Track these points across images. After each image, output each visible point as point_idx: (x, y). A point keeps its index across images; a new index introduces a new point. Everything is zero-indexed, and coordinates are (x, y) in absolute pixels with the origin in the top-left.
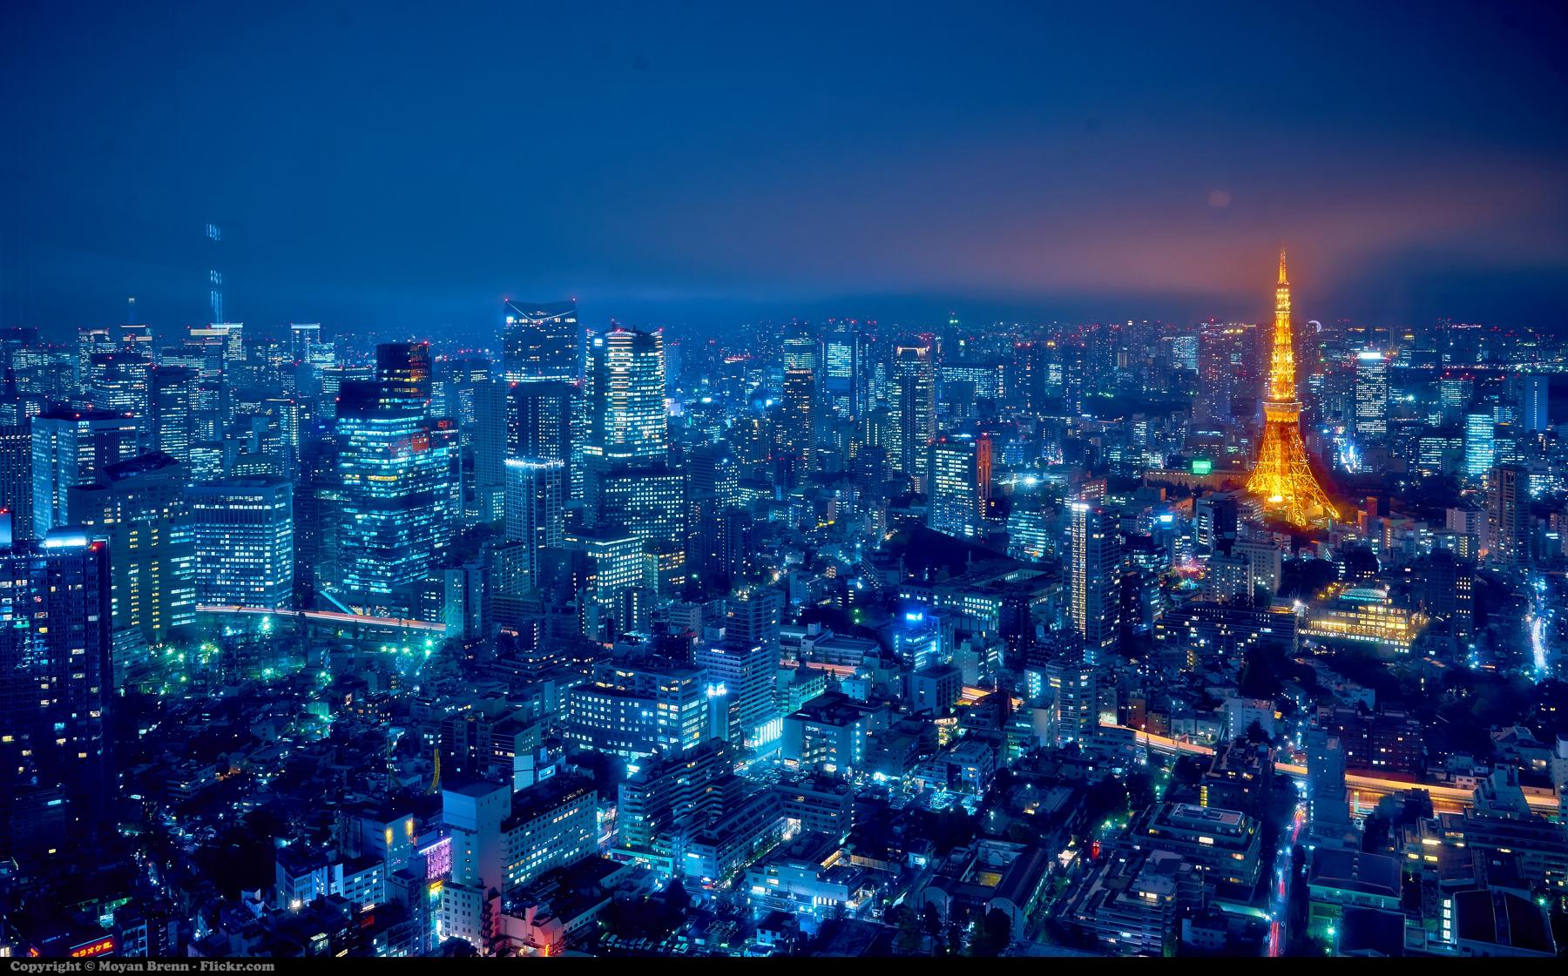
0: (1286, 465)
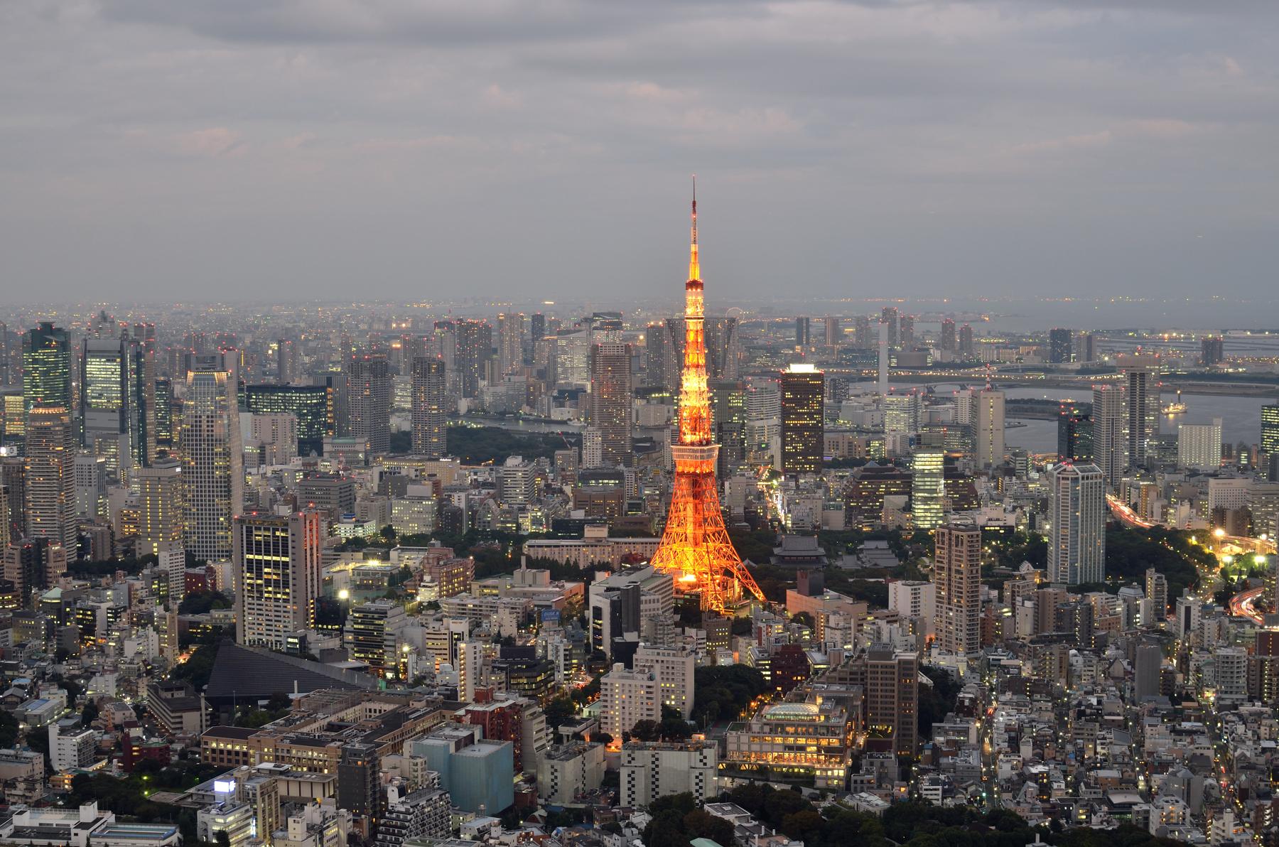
0: (700, 532)
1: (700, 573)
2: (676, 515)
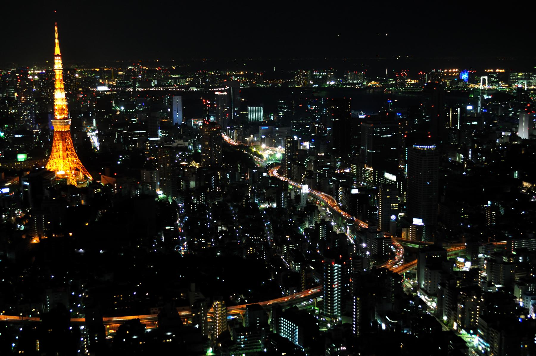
1: (66, 170)
2: (55, 148)
